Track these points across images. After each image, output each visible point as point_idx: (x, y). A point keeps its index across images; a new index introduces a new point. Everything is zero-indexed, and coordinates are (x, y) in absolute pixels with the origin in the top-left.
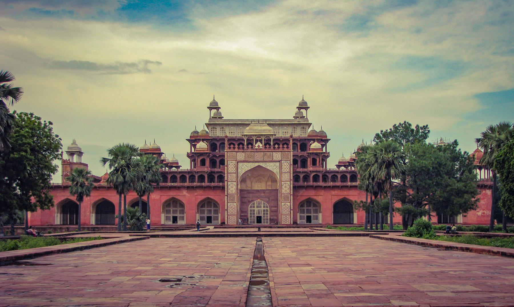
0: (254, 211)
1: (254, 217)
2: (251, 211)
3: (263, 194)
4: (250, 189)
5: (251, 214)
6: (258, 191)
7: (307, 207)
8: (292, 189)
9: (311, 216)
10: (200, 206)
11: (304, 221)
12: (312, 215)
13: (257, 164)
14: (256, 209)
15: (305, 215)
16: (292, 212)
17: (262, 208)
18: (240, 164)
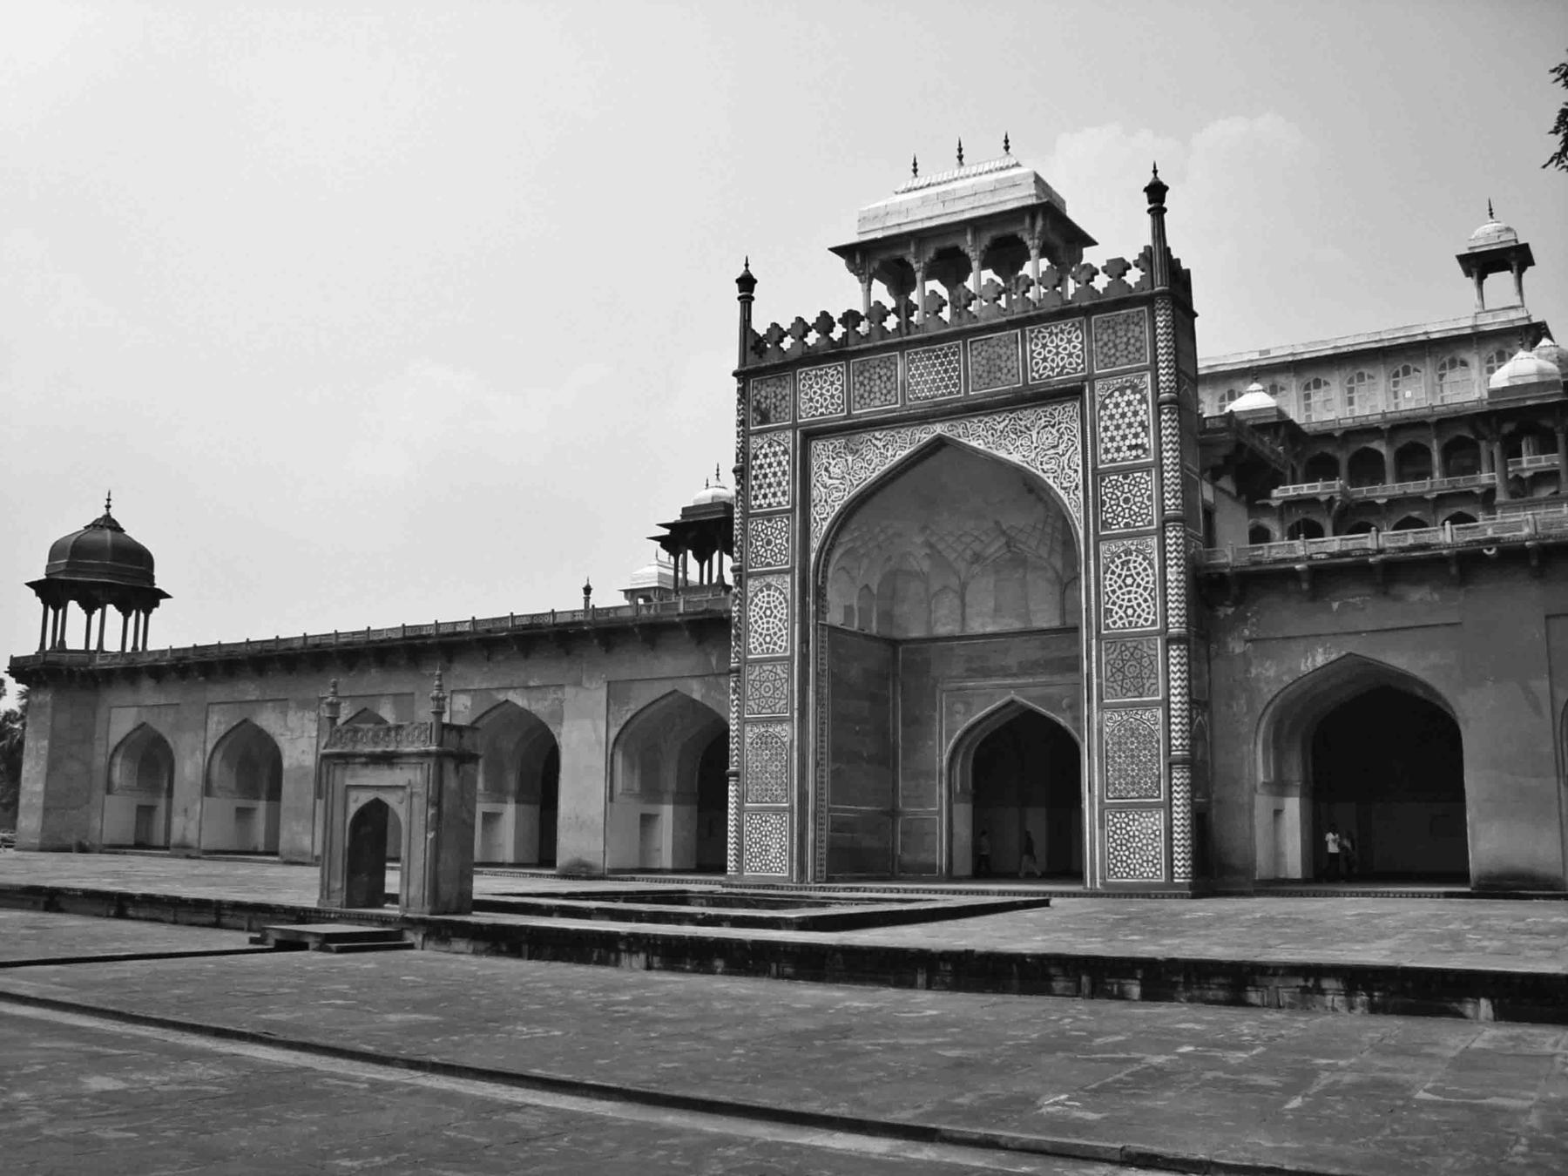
13: (924, 435)
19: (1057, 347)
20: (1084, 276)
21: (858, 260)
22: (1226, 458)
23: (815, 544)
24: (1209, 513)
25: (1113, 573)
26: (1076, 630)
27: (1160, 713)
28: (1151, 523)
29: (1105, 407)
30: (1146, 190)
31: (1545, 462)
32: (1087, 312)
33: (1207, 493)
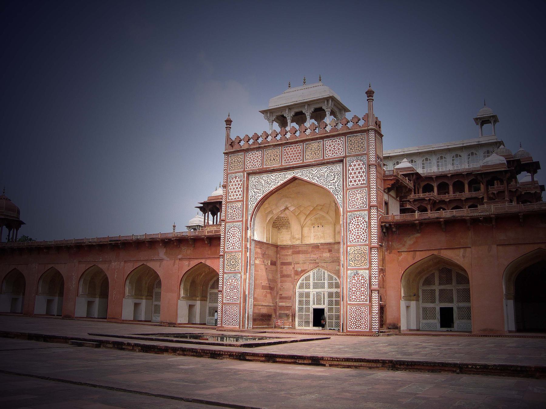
0: (308, 295)
1: (308, 310)
2: (301, 295)
3: (327, 255)
4: (298, 242)
5: (301, 302)
6: (316, 247)
7: (440, 284)
8: (375, 230)
9: (451, 309)
10: (209, 286)
11: (437, 322)
12: (454, 305)
13: (289, 175)
14: (312, 291)
15: (437, 306)
16: (375, 295)
17: (326, 290)
18: (253, 179)
19: (334, 146)
20: (344, 122)
21: (268, 115)
22: (392, 185)
23: (250, 212)
24: (386, 204)
25: (352, 223)
26: (339, 243)
27: (367, 271)
28: (366, 207)
29: (350, 166)
30: (366, 93)
31: (501, 188)
32: (344, 134)
33: (386, 197)
